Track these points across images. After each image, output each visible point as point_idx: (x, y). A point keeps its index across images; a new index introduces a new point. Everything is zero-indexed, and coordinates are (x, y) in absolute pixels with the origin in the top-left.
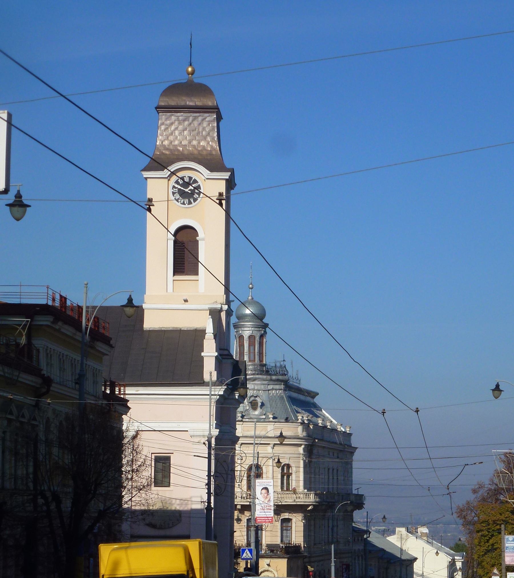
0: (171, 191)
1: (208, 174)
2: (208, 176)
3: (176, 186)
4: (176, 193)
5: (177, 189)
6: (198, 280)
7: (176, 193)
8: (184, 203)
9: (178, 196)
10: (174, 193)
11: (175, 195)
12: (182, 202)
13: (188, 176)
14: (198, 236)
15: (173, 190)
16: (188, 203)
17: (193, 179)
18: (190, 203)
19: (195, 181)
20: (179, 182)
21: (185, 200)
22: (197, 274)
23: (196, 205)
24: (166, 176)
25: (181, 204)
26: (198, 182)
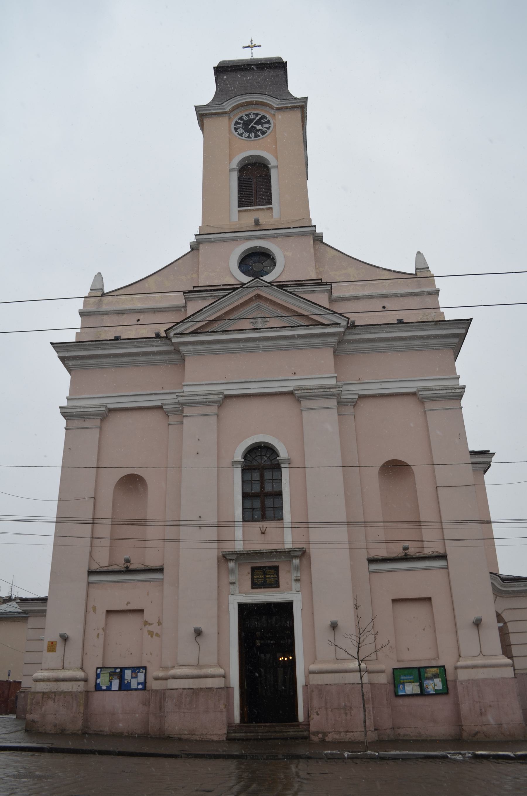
0: (233, 126)
1: (279, 102)
2: (278, 105)
3: (240, 121)
4: (240, 128)
5: (240, 125)
6: (271, 208)
7: (240, 128)
8: (249, 137)
9: (241, 131)
10: (236, 129)
11: (238, 130)
12: (247, 136)
13: (254, 114)
14: (270, 164)
15: (235, 126)
16: (254, 136)
17: (262, 115)
18: (256, 136)
19: (263, 117)
20: (244, 119)
21: (251, 134)
22: (271, 204)
23: (263, 138)
24: (227, 110)
25: (246, 137)
26: (267, 118)
